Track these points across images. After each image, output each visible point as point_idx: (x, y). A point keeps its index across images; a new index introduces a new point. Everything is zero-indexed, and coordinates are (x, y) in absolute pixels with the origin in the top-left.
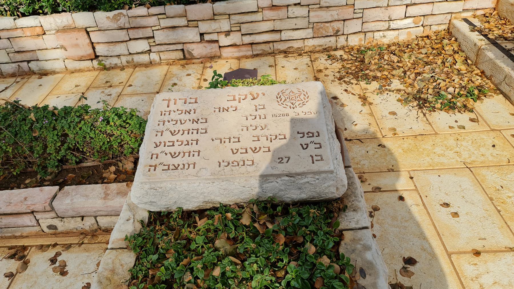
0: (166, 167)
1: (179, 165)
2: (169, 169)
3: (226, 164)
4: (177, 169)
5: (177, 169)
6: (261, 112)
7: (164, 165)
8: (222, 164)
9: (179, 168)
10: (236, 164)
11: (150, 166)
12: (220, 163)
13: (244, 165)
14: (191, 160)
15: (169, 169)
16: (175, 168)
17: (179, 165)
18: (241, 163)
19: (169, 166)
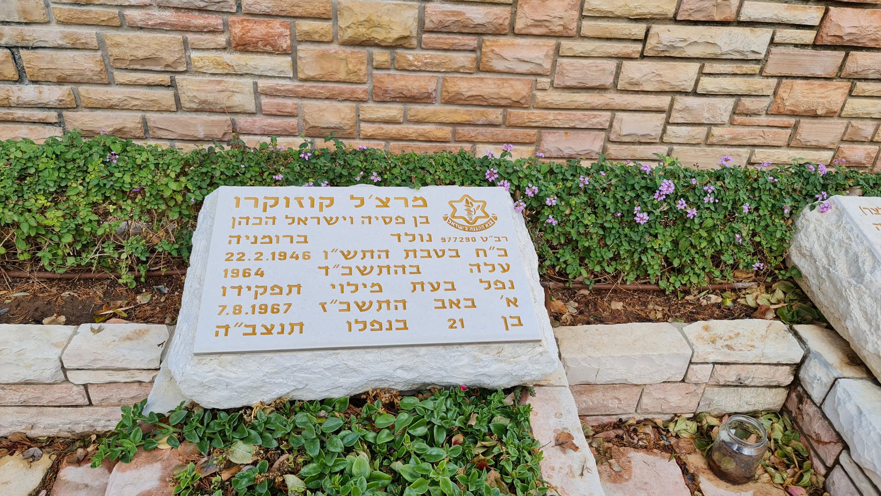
0: (250, 330)
2: (254, 333)
3: (361, 326)
4: (269, 332)
5: (269, 332)
7: (246, 326)
8: (353, 325)
10: (377, 326)
11: (218, 327)
12: (349, 323)
13: (391, 329)
15: (254, 333)
16: (265, 331)
17: (273, 326)
18: (386, 325)
19: (254, 327)
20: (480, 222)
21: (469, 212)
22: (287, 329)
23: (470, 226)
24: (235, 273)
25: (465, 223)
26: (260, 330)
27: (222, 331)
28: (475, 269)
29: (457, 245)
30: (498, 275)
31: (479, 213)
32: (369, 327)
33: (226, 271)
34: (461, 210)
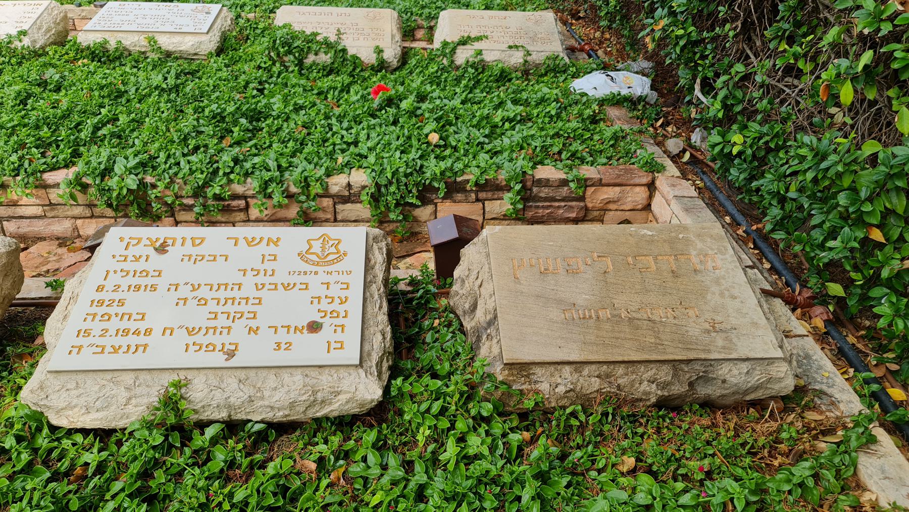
1: (120, 347)
2: (102, 352)
3: (197, 348)
4: (116, 350)
6: (269, 266)
9: (121, 351)
14: (142, 339)
17: (120, 347)
20: (331, 257)
21: (323, 249)
22: (133, 349)
23: (323, 261)
24: (101, 303)
25: (318, 260)
26: (108, 349)
27: (75, 350)
28: (316, 301)
29: (303, 278)
30: (336, 306)
31: (333, 250)
32: (204, 348)
33: (92, 302)
34: (317, 247)
